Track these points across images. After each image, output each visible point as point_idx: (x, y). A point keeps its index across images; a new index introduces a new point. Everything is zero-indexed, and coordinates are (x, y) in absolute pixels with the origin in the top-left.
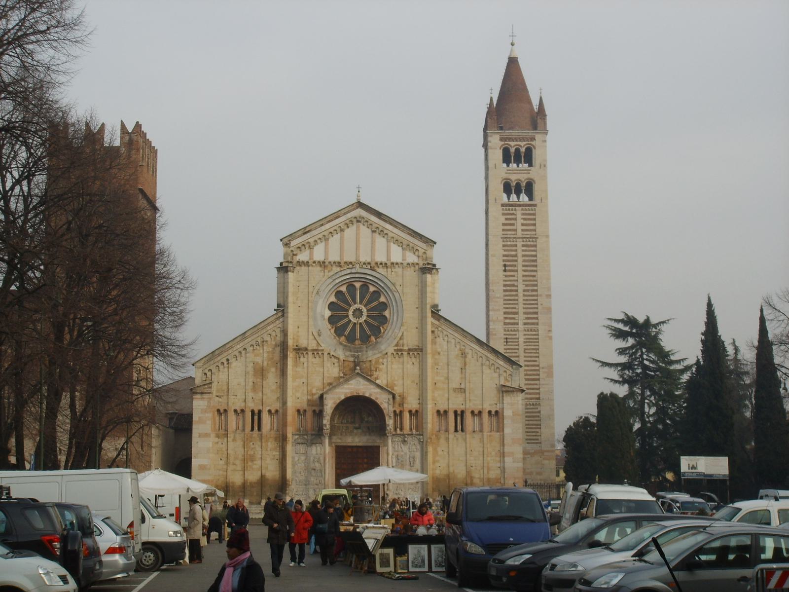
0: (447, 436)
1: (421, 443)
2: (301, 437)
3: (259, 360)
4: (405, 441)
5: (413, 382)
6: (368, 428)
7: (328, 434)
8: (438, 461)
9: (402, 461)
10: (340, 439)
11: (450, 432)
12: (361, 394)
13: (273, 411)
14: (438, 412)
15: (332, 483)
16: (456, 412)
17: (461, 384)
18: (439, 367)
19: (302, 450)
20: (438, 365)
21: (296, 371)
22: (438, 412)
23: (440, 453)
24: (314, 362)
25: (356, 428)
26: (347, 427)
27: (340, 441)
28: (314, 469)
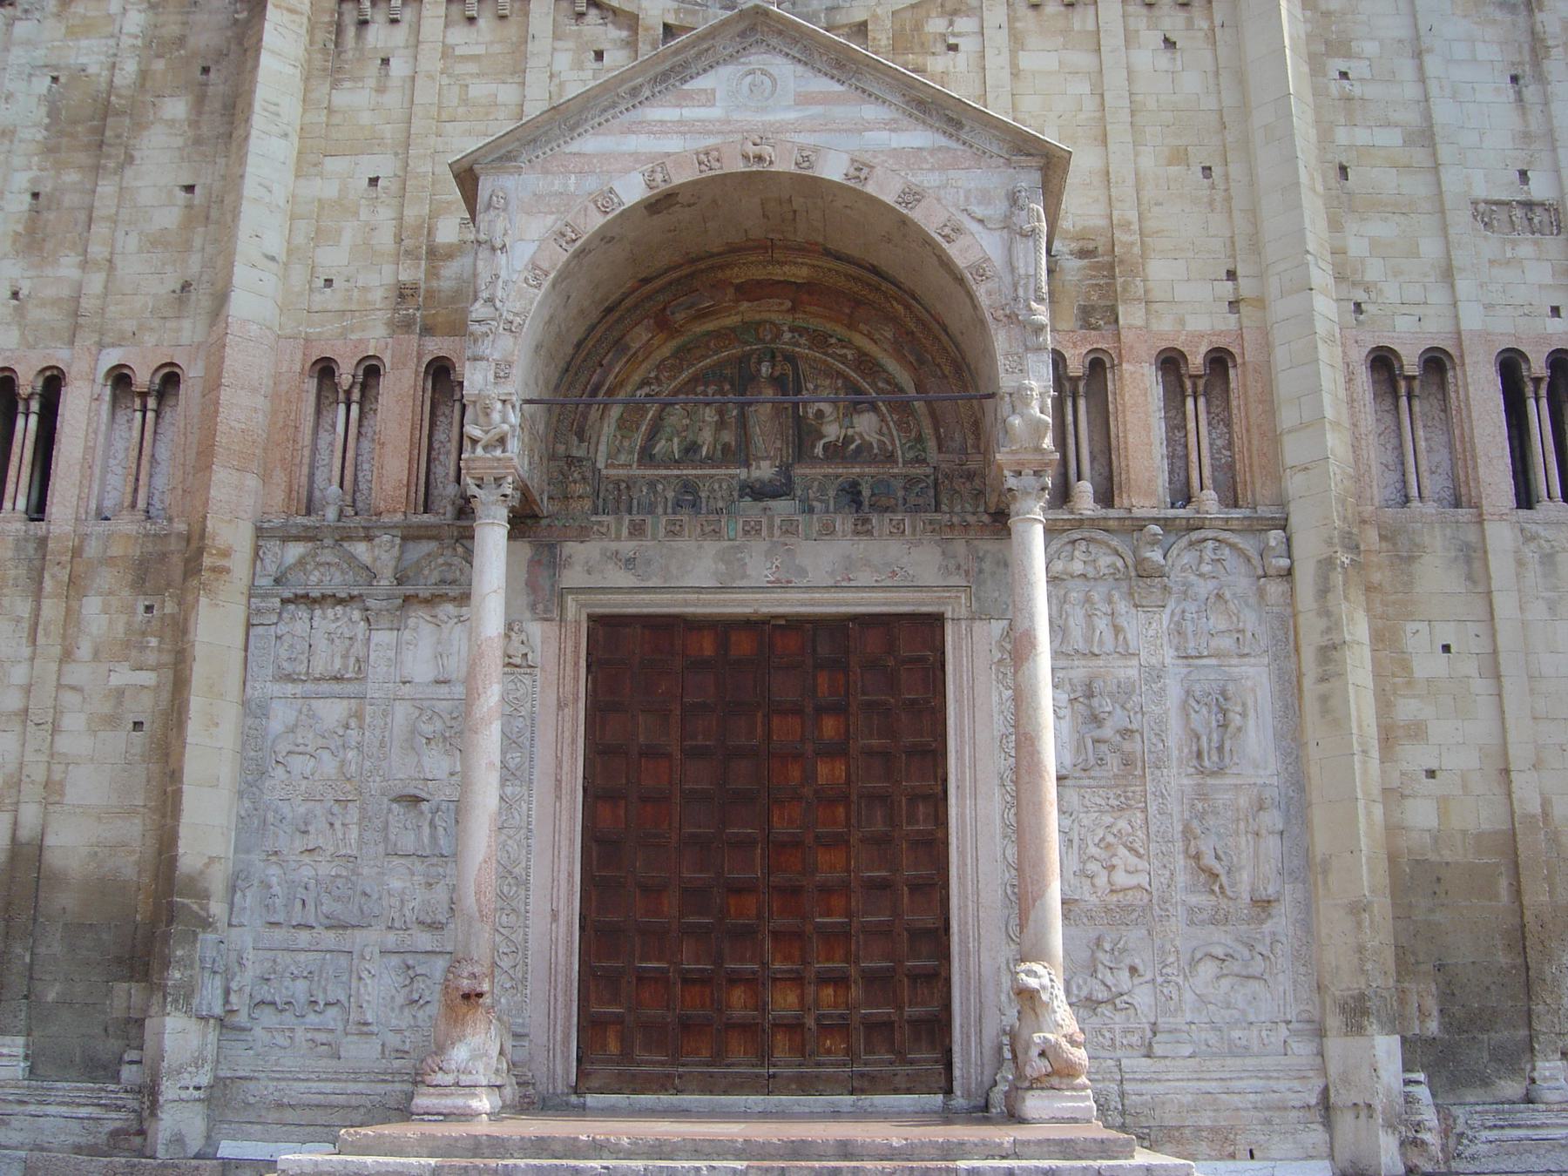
0: (1472, 536)
1: (1275, 589)
2: (327, 556)
3: (89, 55)
4: (1144, 572)
5: (1179, 156)
6: (852, 495)
7: (498, 481)
8: (1417, 731)
9: (1126, 733)
10: (630, 563)
11: (1487, 507)
12: (784, 164)
13: (143, 378)
14: (1383, 362)
15: (555, 915)
16: (1510, 366)
17: (1523, 174)
18: (1356, 68)
19: (321, 644)
20: (1348, 56)
21: (330, 110)
22: (1383, 362)
23: (1428, 665)
24: (458, 52)
25: (758, 492)
26: (689, 487)
27: (625, 579)
28: (416, 800)
